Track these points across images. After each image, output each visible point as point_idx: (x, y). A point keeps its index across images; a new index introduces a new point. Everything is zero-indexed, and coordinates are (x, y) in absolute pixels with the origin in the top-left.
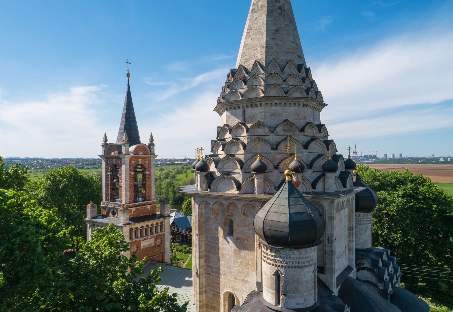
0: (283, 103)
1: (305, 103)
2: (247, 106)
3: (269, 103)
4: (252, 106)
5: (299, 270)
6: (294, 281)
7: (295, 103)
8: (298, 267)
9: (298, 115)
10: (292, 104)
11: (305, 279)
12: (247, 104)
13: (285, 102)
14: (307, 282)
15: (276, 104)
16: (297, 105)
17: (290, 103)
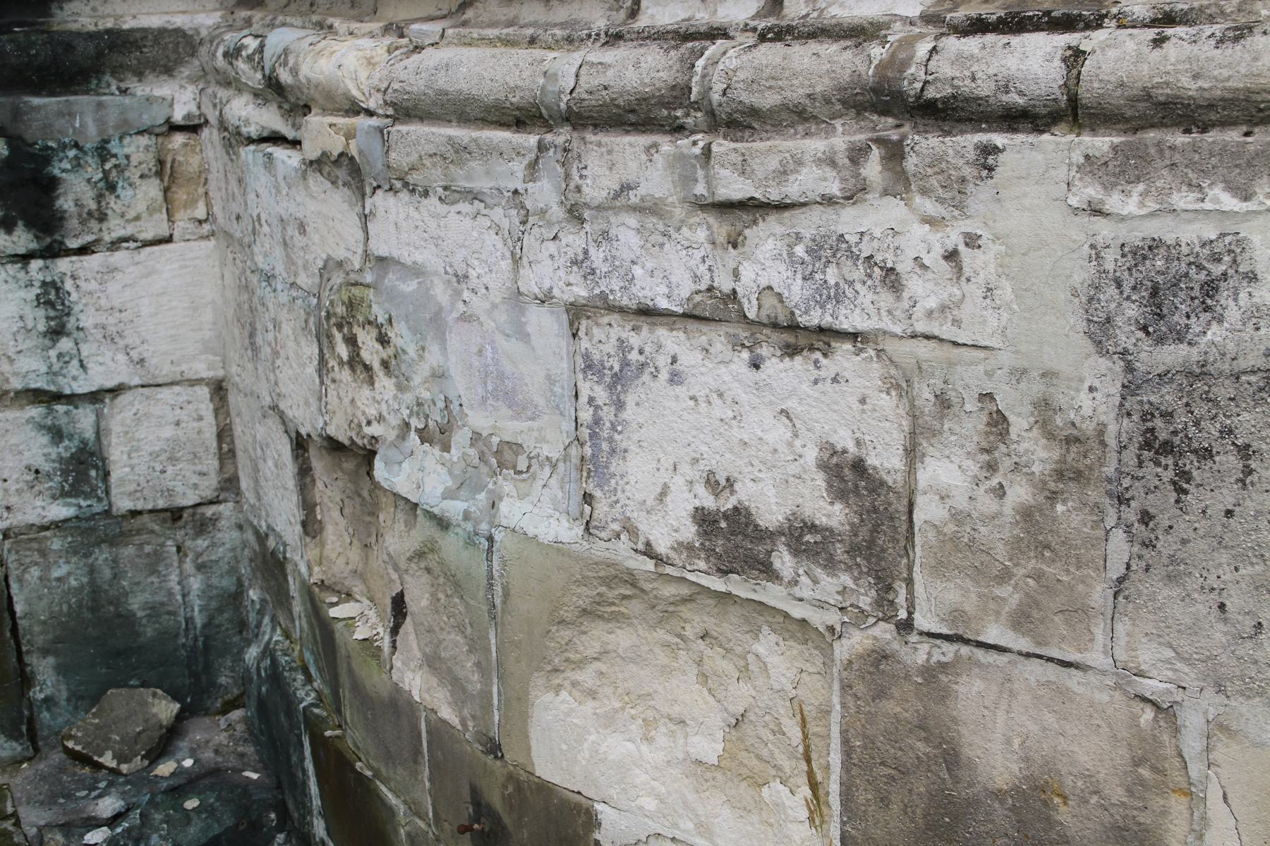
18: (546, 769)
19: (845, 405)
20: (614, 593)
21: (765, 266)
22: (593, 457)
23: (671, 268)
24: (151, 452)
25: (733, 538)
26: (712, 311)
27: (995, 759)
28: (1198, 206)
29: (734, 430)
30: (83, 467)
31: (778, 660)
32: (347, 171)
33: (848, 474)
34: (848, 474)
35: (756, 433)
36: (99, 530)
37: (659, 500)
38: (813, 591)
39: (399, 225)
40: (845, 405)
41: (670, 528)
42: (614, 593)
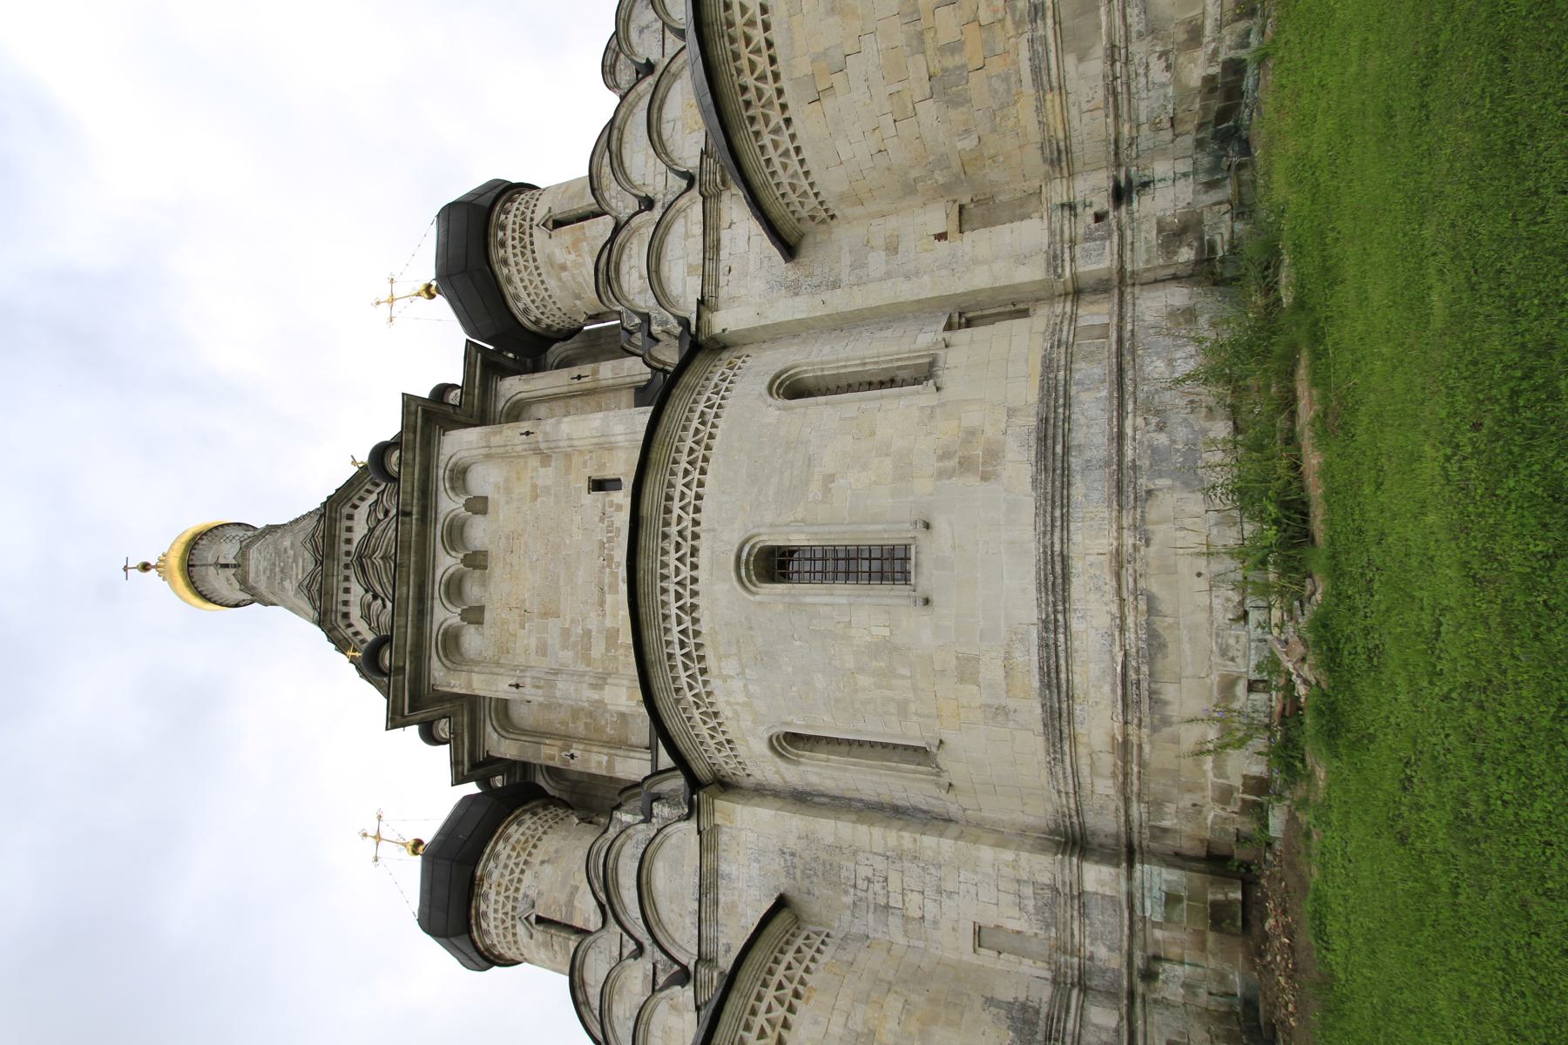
18: (1199, 83)
19: (1153, 60)
20: (1177, 80)
21: (1141, 71)
22: (1163, 85)
23: (1142, 80)
24: (1183, 166)
25: (1168, 68)
26: (1146, 75)
27: (1185, 36)
28: (1134, 35)
29: (1158, 72)
30: (1185, 175)
31: (1181, 60)
32: (1138, 126)
33: (1160, 58)
34: (1160, 58)
35: (1157, 66)
36: (1195, 172)
37: (1164, 77)
38: (1172, 58)
39: (1143, 118)
40: (1153, 60)
41: (1168, 75)
42: (1177, 80)
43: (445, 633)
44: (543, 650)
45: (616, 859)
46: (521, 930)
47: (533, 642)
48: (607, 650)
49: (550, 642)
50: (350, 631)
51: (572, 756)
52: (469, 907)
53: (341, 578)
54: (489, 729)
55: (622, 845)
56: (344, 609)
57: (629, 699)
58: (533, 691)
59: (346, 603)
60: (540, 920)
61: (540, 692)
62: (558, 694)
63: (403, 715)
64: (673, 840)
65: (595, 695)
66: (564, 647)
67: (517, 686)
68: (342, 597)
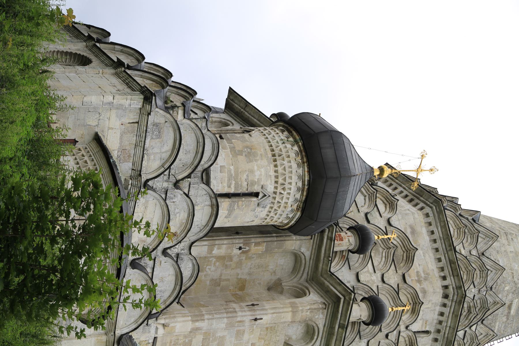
0: (438, 245)
1: (451, 288)
2: (406, 196)
3: (431, 219)
4: (411, 201)
5: (270, 155)
6: (251, 149)
7: (446, 268)
8: (274, 155)
9: (426, 279)
10: (441, 264)
11: (256, 168)
12: (409, 194)
13: (440, 249)
14: (252, 171)
15: (432, 233)
16: (443, 275)
17: (443, 258)
43: (312, 339)
44: (239, 334)
45: (174, 289)
46: (270, 188)
47: (246, 337)
48: (191, 341)
49: (233, 339)
50: (446, 283)
51: (240, 248)
52: (307, 196)
53: (444, 324)
54: (307, 254)
55: (170, 296)
56: (446, 301)
57: (174, 327)
58: (244, 319)
59: (445, 305)
60: (256, 195)
61: (239, 319)
62: (225, 320)
63: (345, 299)
64: (133, 320)
65: (198, 324)
66: (223, 338)
67: (256, 320)
68: (446, 310)
